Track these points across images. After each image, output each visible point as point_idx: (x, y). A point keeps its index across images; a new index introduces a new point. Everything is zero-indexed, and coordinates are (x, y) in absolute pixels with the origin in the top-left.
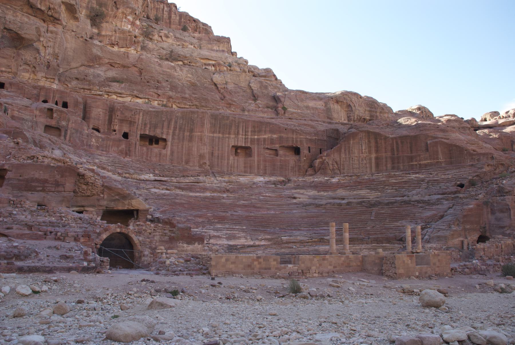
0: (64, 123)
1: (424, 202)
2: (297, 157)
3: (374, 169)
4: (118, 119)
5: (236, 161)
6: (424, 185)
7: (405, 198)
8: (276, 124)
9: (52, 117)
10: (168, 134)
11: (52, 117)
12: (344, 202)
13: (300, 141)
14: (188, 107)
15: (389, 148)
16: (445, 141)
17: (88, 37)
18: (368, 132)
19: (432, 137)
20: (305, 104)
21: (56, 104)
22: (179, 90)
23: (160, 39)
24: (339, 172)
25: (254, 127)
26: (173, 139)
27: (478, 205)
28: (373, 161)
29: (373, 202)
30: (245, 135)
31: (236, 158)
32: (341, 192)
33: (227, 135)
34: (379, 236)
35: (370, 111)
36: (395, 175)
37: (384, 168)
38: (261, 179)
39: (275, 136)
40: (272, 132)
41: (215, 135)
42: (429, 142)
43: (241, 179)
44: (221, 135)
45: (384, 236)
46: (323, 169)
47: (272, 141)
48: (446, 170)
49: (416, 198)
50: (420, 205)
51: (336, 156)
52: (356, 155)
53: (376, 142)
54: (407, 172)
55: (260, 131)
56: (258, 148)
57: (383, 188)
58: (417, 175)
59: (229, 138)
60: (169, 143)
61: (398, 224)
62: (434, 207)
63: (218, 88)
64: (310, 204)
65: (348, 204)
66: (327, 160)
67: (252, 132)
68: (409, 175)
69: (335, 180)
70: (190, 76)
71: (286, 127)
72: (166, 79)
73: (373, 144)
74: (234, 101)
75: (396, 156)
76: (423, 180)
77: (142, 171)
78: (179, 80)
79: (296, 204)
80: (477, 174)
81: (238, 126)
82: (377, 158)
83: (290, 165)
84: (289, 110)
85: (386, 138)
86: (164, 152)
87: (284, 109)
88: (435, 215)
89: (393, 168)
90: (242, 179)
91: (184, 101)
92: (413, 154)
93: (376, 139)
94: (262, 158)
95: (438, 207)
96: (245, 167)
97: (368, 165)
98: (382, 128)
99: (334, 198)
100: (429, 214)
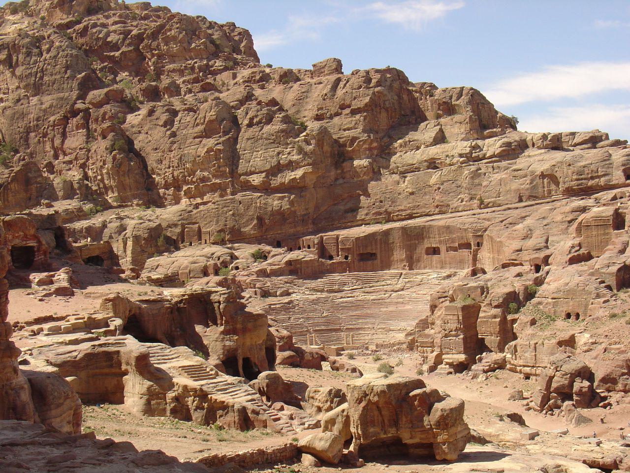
0: (299, 266)
9: (291, 265)
10: (376, 249)
11: (291, 265)
17: (334, 180)
20: (508, 188)
22: (397, 204)
25: (439, 230)
26: (381, 251)
35: (577, 180)
41: (412, 242)
60: (379, 256)
67: (438, 234)
72: (388, 196)
77: (346, 285)
78: (400, 194)
86: (375, 262)
87: (482, 202)
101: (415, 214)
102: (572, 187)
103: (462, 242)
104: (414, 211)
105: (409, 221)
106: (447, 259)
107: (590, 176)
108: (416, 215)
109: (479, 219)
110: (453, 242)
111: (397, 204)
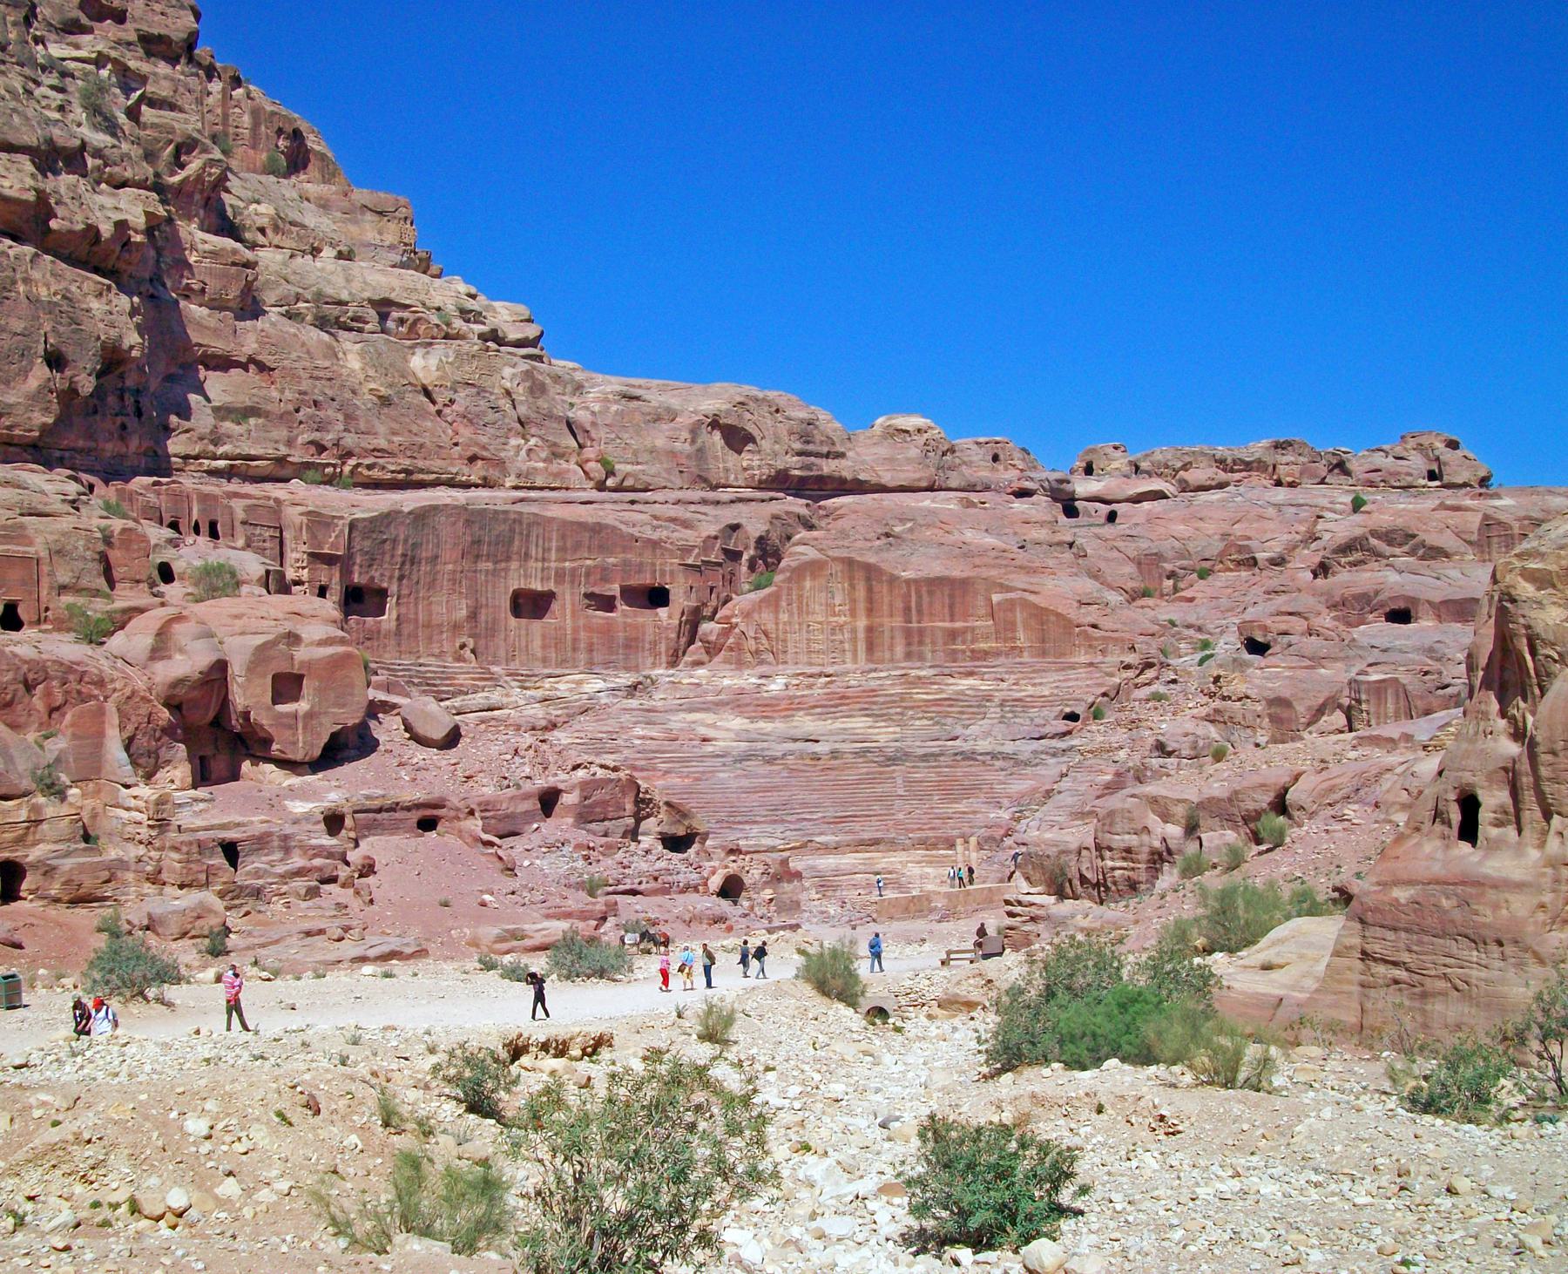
1: (1006, 757)
2: (662, 612)
3: (862, 654)
4: (311, 555)
5: (523, 632)
6: (994, 711)
7: (957, 743)
8: (614, 528)
10: (391, 578)
12: (817, 748)
13: (672, 572)
14: (389, 476)
15: (899, 604)
16: (1032, 598)
18: (849, 563)
19: (1001, 585)
20: (648, 443)
21: (197, 530)
23: (261, 239)
24: (770, 658)
25: (563, 537)
27: (1118, 774)
28: (861, 635)
29: (890, 751)
30: (544, 560)
31: (524, 621)
32: (806, 724)
33: (503, 565)
34: (930, 834)
36: (919, 678)
37: (887, 655)
38: (600, 685)
39: (611, 560)
40: (602, 548)
42: (996, 598)
43: (562, 686)
44: (490, 565)
45: (938, 833)
46: (731, 649)
47: (605, 574)
48: (1034, 672)
49: (984, 745)
50: (998, 764)
51: (766, 618)
52: (820, 619)
53: (870, 590)
54: (947, 671)
55: (577, 546)
56: (572, 594)
57: (902, 714)
58: (971, 681)
59: (506, 570)
60: (391, 602)
61: (961, 807)
62: (1029, 770)
63: (434, 402)
64: (746, 757)
65: (835, 754)
66: (742, 627)
67: (559, 549)
68: (951, 681)
69: (776, 686)
70: (371, 373)
71: (635, 531)
73: (861, 593)
74: (484, 448)
75: (915, 625)
76: (989, 698)
79: (718, 756)
80: (1103, 690)
81: (528, 536)
82: (870, 630)
83: (648, 638)
84: (617, 467)
85: (893, 580)
88: (1035, 790)
89: (908, 656)
90: (563, 687)
91: (381, 461)
92: (958, 625)
93: (868, 579)
94: (581, 622)
95: (1040, 770)
96: (544, 647)
97: (847, 646)
98: (880, 549)
99: (796, 740)
100: (1019, 786)
101: (421, 471)
102: (786, 470)
103: (635, 581)
104: (420, 464)
105: (483, 493)
106: (583, 635)
107: (825, 449)
108: (425, 477)
109: (655, 517)
110: (605, 579)
111: (362, 426)
